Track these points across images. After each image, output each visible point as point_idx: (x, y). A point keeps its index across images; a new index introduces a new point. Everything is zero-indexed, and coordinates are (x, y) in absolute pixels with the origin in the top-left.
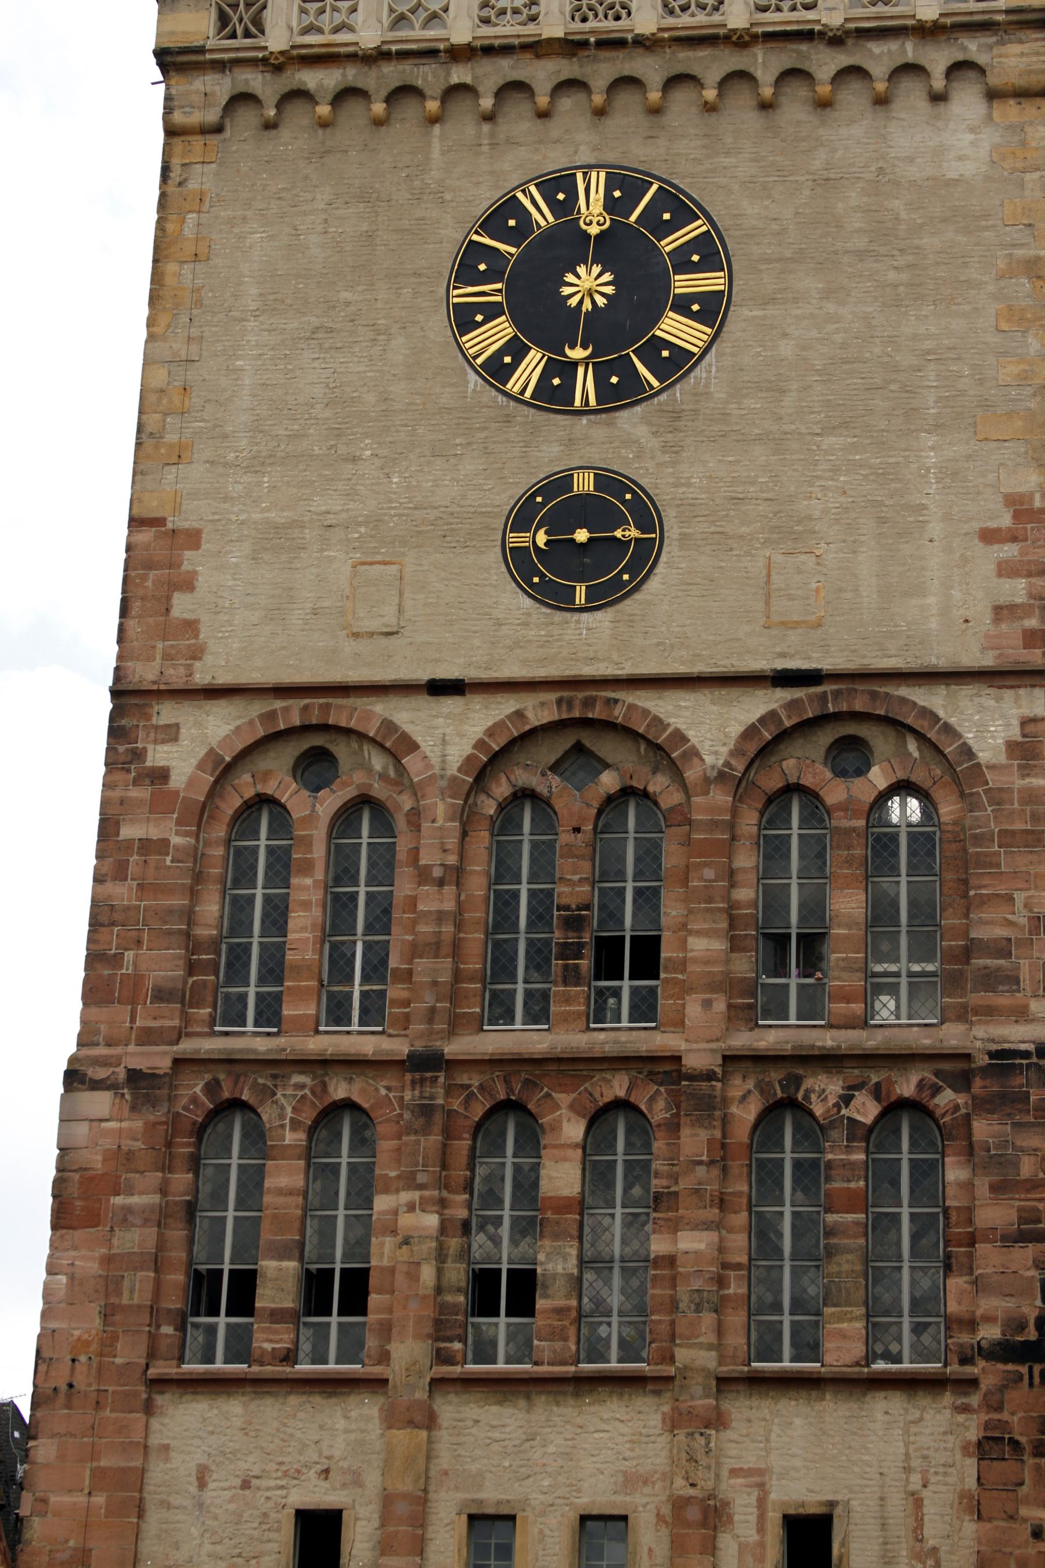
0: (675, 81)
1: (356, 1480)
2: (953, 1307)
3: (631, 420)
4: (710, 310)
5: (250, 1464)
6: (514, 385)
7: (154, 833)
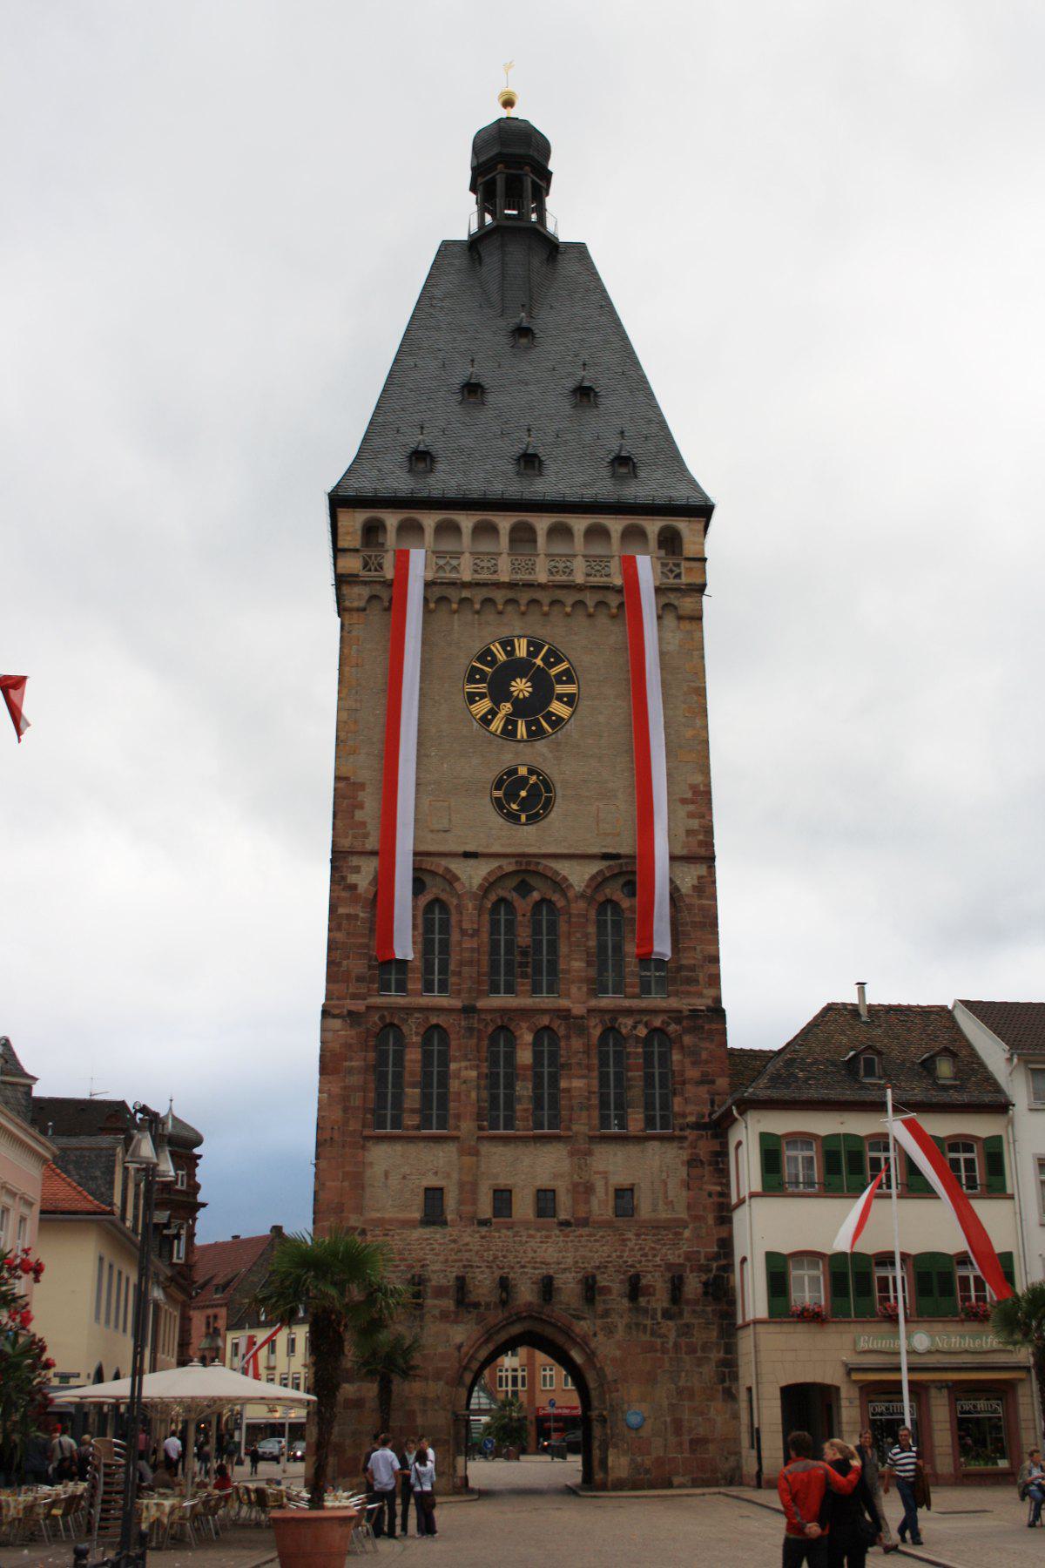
0: (553, 603)
1: (448, 1176)
2: (676, 1109)
3: (541, 746)
4: (570, 700)
5: (406, 1169)
6: (493, 727)
7: (351, 911)
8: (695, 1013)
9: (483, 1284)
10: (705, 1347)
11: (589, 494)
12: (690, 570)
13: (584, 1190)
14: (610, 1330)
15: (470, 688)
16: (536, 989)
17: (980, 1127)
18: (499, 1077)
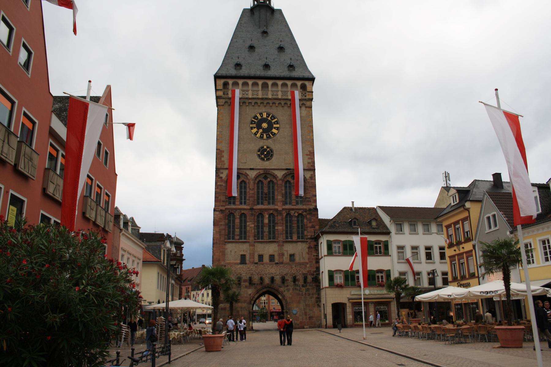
0: (273, 103)
3: (270, 141)
4: (278, 129)
5: (236, 250)
6: (257, 136)
8: (310, 209)
9: (256, 279)
10: (312, 294)
11: (282, 75)
12: (309, 95)
13: (281, 255)
14: (288, 290)
15: (251, 126)
16: (269, 204)
17: (383, 238)
18: (259, 227)
